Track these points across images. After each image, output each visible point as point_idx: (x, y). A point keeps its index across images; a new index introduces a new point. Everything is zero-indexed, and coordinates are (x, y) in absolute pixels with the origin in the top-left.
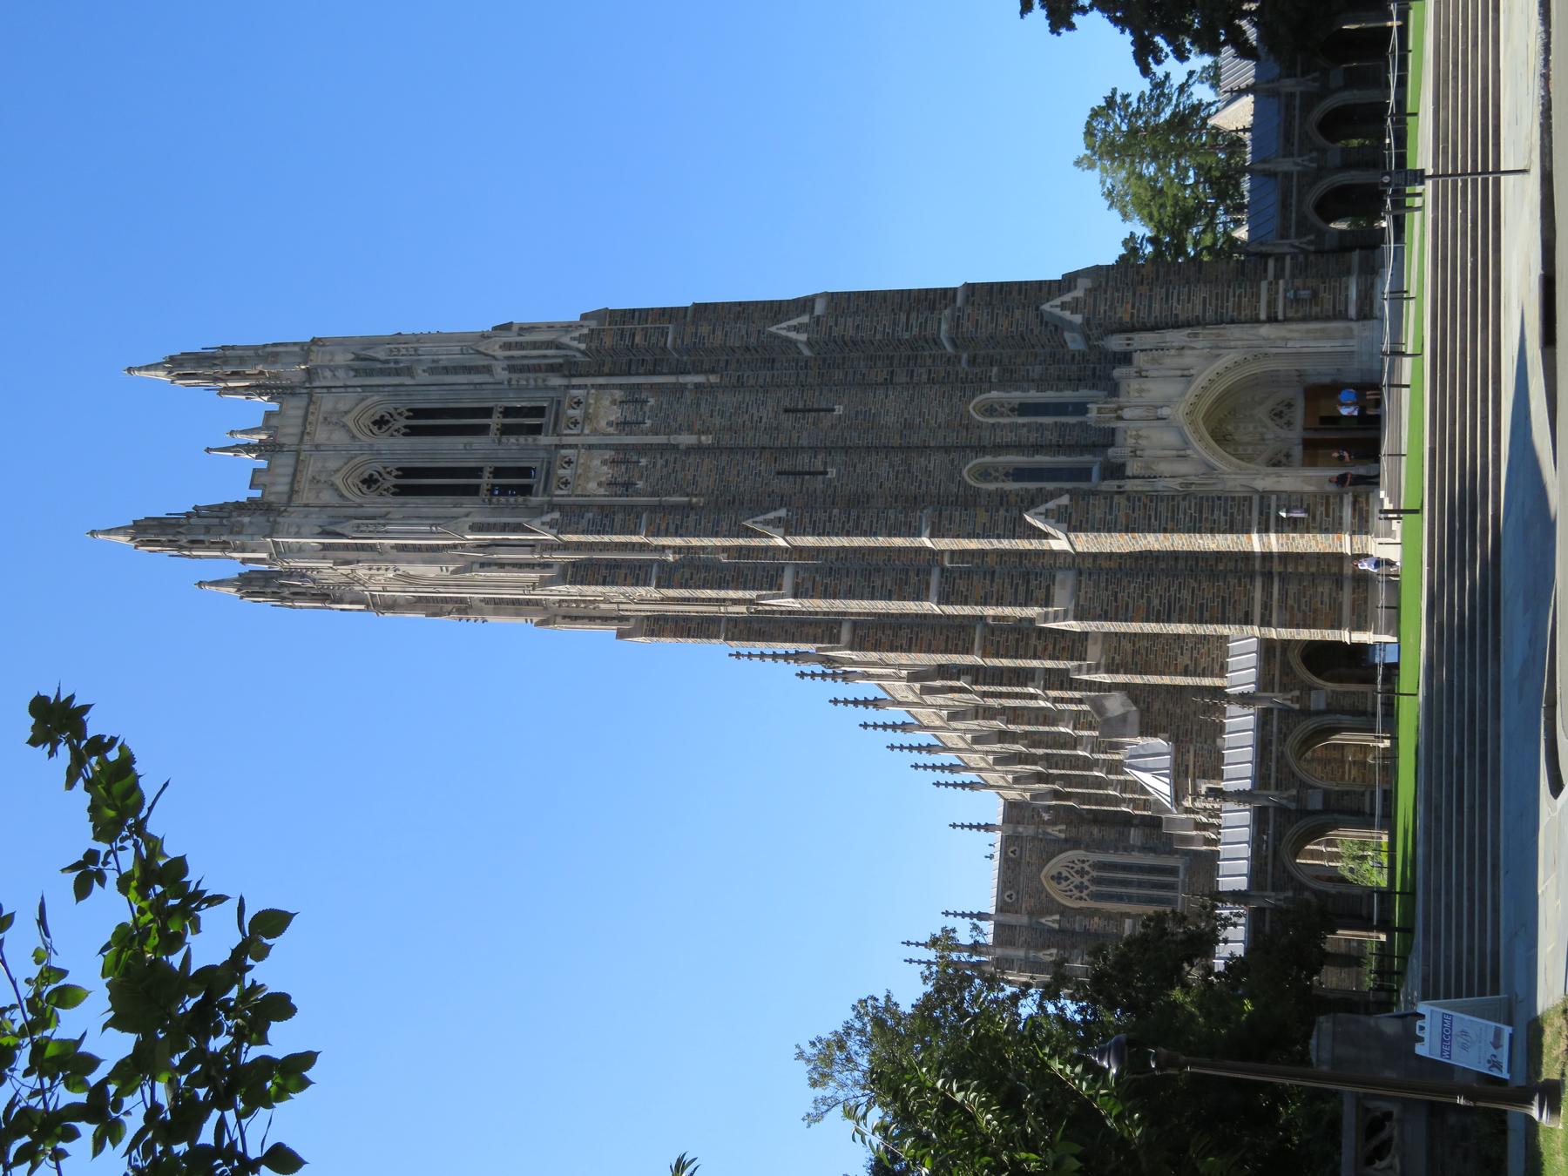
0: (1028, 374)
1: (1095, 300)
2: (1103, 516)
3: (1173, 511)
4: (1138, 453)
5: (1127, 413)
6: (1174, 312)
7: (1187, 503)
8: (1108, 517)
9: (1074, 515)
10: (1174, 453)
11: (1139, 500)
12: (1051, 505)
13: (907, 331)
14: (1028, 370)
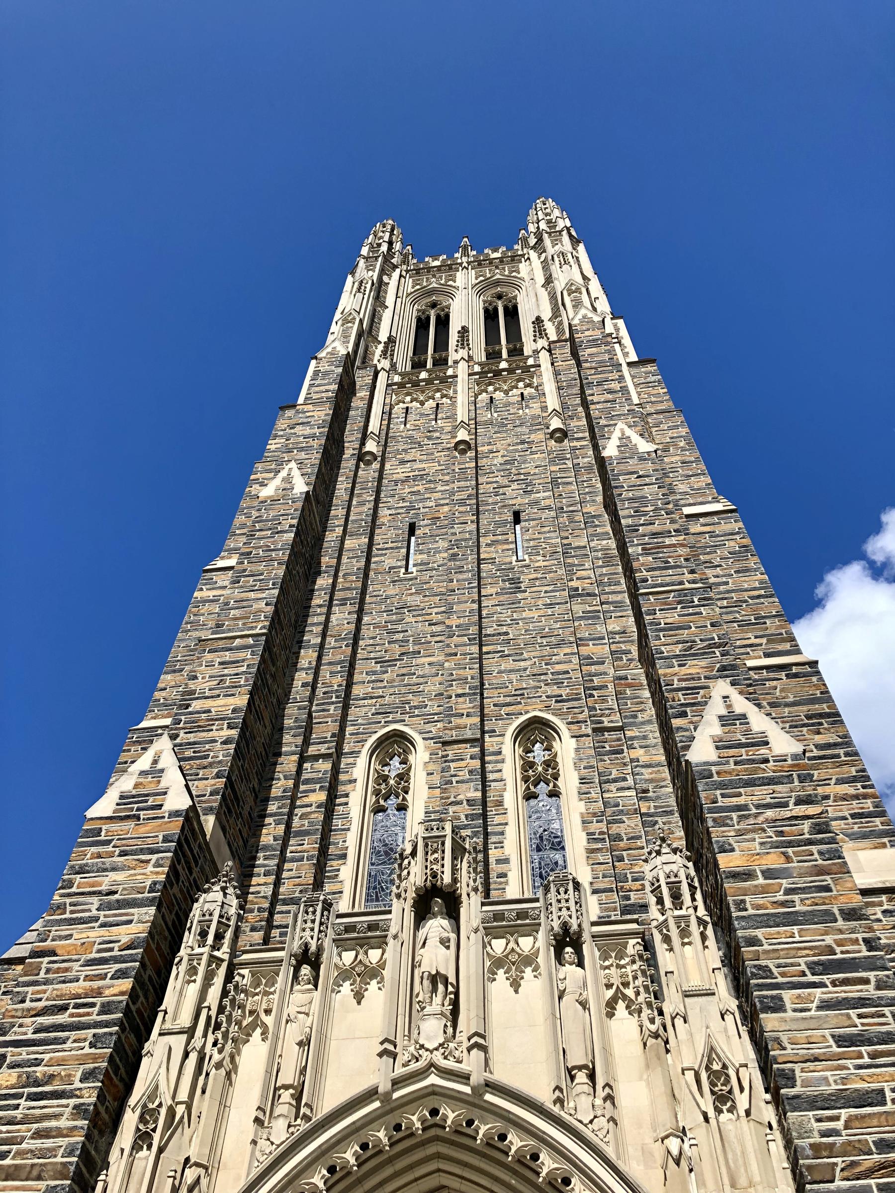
0: (615, 781)
1: (771, 781)
2: (104, 888)
3: (50, 1078)
4: (306, 970)
5: (437, 926)
6: (788, 996)
7: (64, 1123)
8: (95, 901)
9: (131, 824)
10: (288, 1076)
11: (120, 975)
12: (173, 779)
13: (643, 549)
14: (625, 779)
